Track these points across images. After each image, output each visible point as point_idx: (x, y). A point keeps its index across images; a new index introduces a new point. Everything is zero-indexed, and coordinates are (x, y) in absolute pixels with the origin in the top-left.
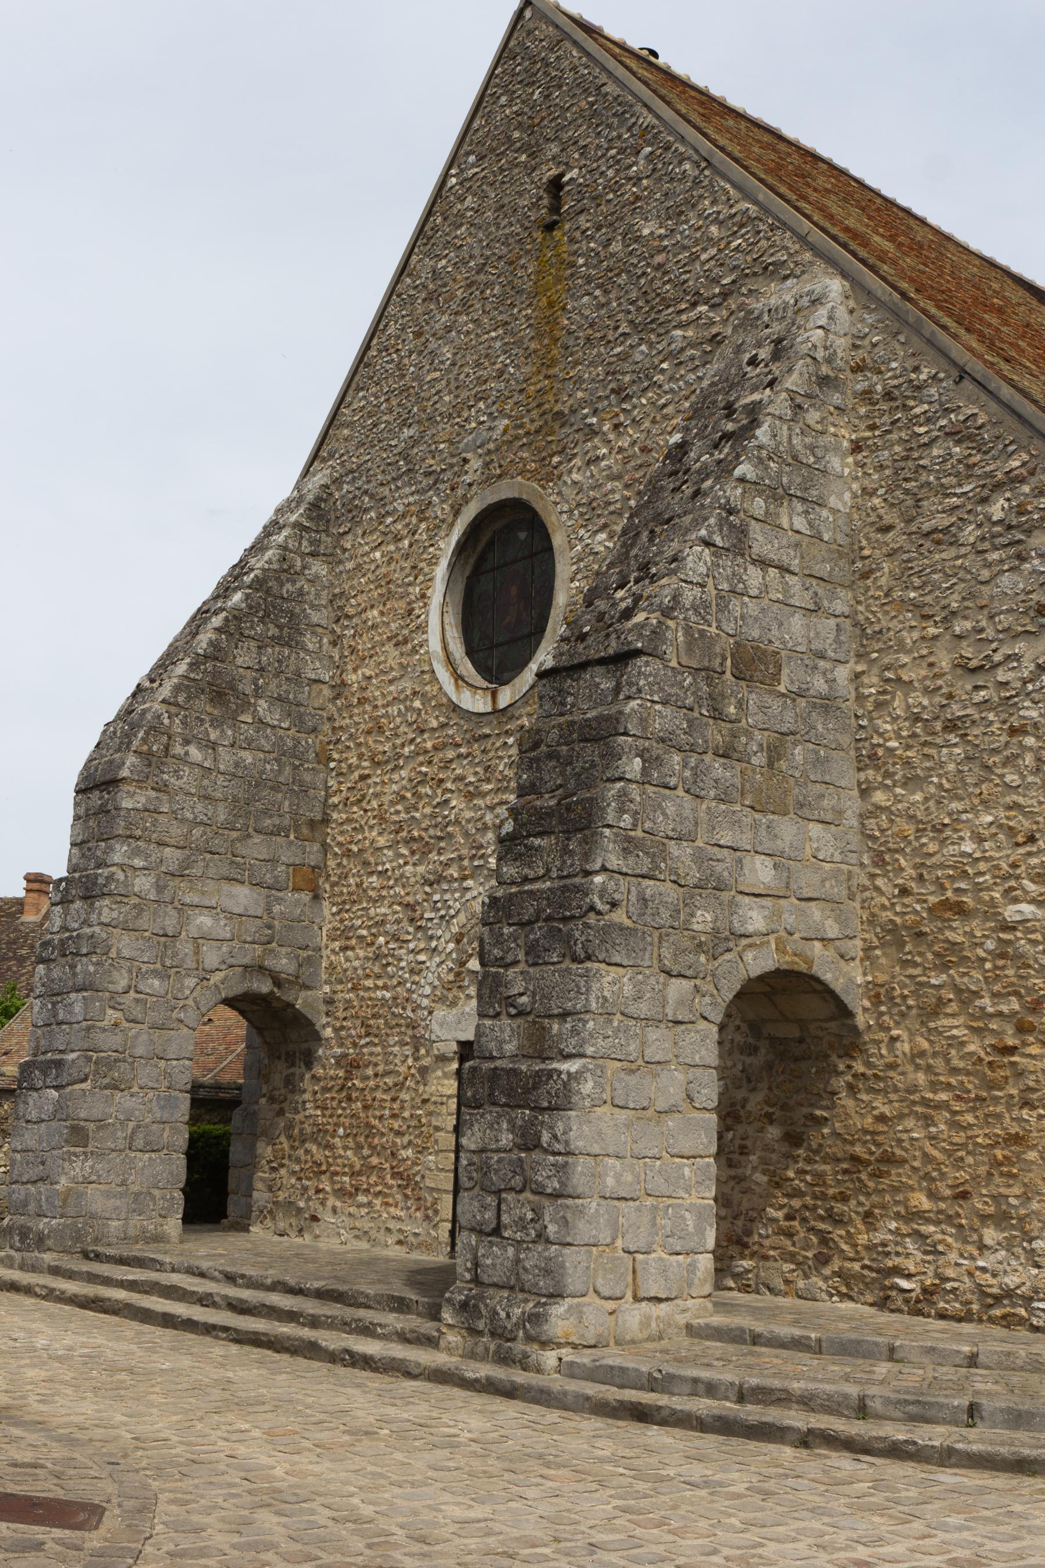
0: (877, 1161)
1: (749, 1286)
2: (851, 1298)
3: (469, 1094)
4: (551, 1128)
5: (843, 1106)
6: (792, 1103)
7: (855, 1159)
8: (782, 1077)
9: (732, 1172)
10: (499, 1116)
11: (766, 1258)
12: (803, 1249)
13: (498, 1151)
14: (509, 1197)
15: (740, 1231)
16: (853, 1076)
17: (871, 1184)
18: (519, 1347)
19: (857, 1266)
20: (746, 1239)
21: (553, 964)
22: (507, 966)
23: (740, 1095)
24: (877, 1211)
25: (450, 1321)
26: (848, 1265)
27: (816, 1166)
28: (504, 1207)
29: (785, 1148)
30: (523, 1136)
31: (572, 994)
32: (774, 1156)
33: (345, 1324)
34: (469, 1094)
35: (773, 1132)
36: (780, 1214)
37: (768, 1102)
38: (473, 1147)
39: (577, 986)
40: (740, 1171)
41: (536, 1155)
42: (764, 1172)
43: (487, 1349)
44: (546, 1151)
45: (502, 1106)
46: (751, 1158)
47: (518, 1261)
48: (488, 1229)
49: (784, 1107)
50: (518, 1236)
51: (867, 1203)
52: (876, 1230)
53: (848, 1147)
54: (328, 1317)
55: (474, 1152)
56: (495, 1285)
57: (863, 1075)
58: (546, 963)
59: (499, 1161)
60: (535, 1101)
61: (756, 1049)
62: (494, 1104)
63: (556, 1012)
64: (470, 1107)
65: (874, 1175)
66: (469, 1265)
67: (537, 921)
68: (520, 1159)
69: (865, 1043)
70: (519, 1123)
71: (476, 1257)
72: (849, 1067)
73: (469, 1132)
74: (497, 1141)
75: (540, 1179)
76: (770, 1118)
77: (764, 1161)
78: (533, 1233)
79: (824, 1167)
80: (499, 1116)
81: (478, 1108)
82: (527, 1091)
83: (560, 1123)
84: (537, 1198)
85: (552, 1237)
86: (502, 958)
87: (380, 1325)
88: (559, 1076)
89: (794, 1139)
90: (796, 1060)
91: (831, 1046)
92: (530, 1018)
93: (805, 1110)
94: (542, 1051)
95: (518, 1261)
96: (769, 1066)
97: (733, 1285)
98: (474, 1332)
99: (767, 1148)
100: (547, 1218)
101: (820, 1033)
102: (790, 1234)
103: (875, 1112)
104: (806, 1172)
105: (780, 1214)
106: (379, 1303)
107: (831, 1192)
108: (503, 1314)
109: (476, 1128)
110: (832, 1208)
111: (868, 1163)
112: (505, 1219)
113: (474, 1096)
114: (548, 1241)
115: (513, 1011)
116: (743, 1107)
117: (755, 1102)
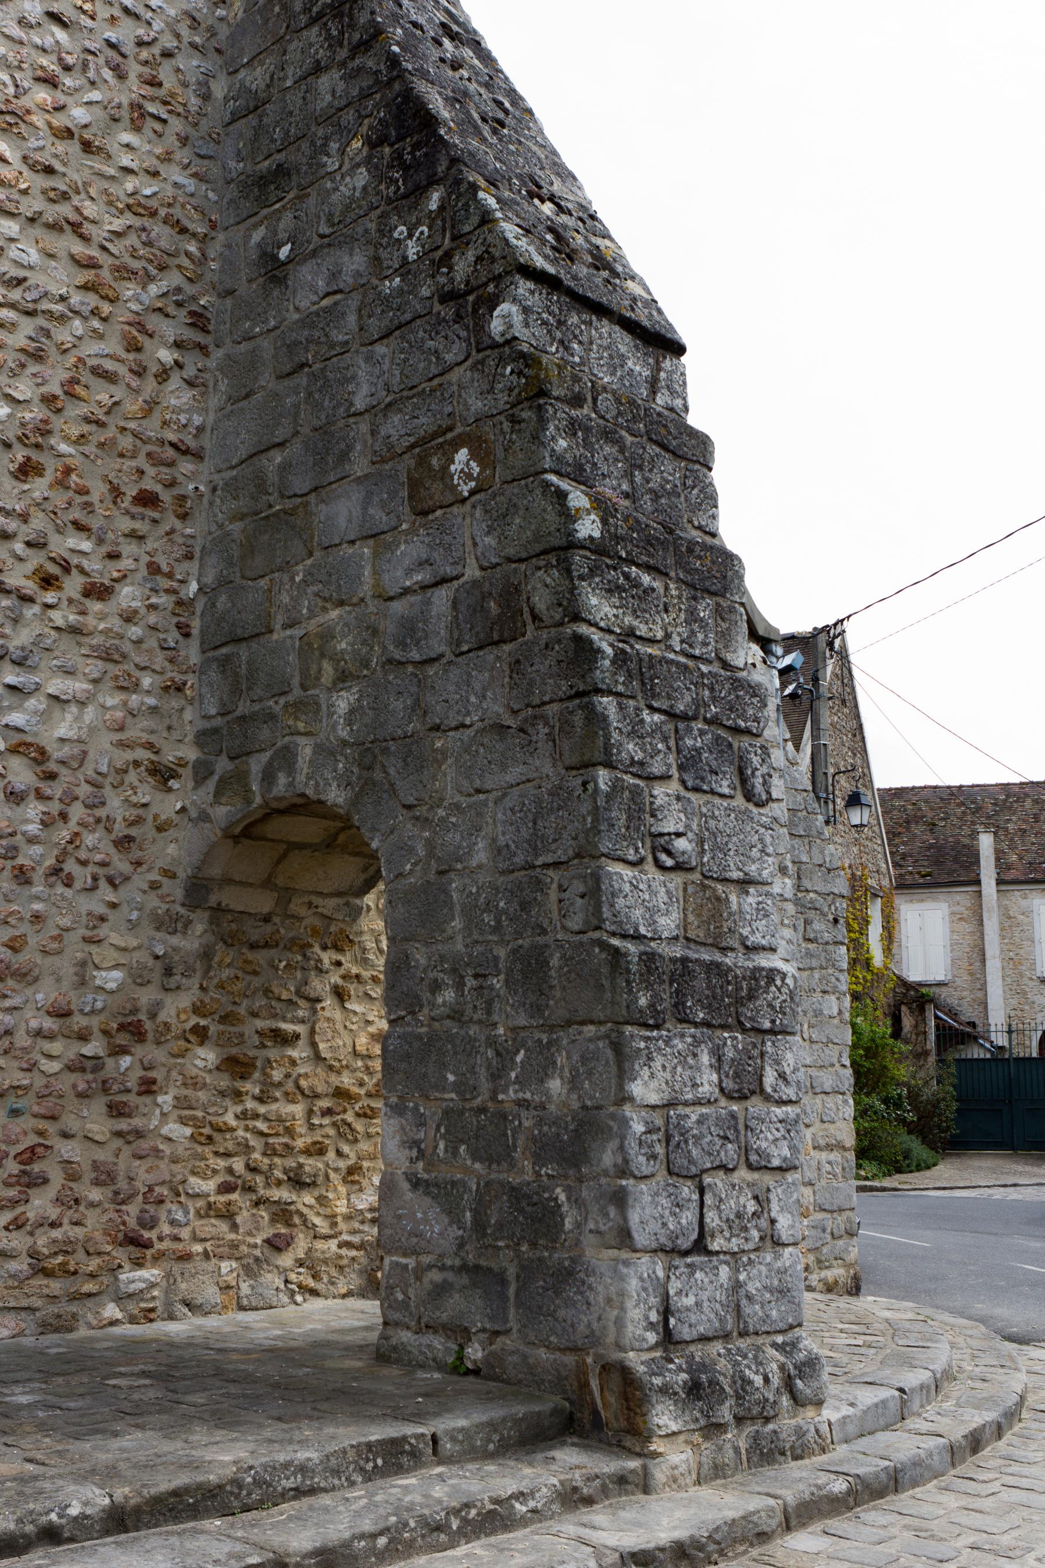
0: (369, 1095)
1: (152, 1310)
2: (314, 1293)
3: (643, 1002)
4: (778, 1062)
5: (328, 1020)
6: (242, 1010)
7: (340, 1093)
8: (226, 973)
9: (123, 1125)
10: (697, 1042)
11: (186, 1257)
12: (250, 1234)
13: (698, 1102)
14: (716, 1181)
15: (132, 1222)
16: (344, 977)
17: (359, 1126)
18: (787, 1423)
19: (333, 1245)
20: (146, 1234)
21: (722, 796)
22: (651, 778)
23: (146, 996)
24: (365, 1164)
25: (674, 1427)
26: (320, 1245)
27: (274, 1107)
28: (709, 1200)
29: (224, 1082)
30: (737, 1075)
31: (755, 853)
32: (202, 1095)
33: (438, 1528)
34: (643, 1002)
35: (206, 1056)
36: (209, 1186)
37: (197, 1010)
38: (654, 1099)
39: (761, 840)
40: (137, 1122)
41: (755, 1106)
42: (183, 1121)
43: (737, 1450)
44: (767, 1098)
45: (696, 1025)
46: (160, 1099)
47: (737, 1286)
48: (685, 1244)
49: (226, 1019)
50: (734, 1244)
51: (352, 1155)
52: (361, 1190)
53: (334, 1079)
54: (374, 1536)
55: (654, 1107)
56: (704, 1339)
57: (357, 976)
58: (713, 792)
59: (699, 1122)
60: (752, 1019)
61: (188, 923)
62: (684, 1021)
63: (735, 875)
64: (646, 1026)
65: (365, 1115)
66: (654, 1317)
67: (695, 718)
68: (733, 1116)
69: (361, 933)
70: (729, 1053)
71: (666, 1297)
72: (339, 964)
73: (645, 1072)
74: (695, 1085)
75: (764, 1145)
76: (201, 1034)
77: (181, 1103)
78: (755, 1234)
79: (291, 1108)
80: (697, 1042)
81: (657, 1027)
82: (739, 1001)
83: (789, 1055)
84: (756, 1175)
85: (784, 1238)
86: (641, 764)
87: (521, 1496)
88: (783, 980)
89: (237, 1066)
90: (253, 947)
91: (315, 932)
92: (696, 876)
93: (260, 1024)
94: (720, 935)
95: (737, 1286)
96: (206, 955)
97: (119, 1315)
98: (713, 1429)
99: (193, 1083)
100: (775, 1206)
101: (303, 911)
102: (228, 1215)
103: (371, 1029)
104: (256, 1116)
105: (209, 1186)
106: (336, 1473)
107: (300, 1143)
108: (758, 1380)
109: (657, 1064)
110: (301, 1166)
111: (356, 1098)
112: (712, 1219)
113: (652, 1005)
114: (778, 1243)
115: (669, 862)
116: (153, 1016)
117: (176, 1008)
